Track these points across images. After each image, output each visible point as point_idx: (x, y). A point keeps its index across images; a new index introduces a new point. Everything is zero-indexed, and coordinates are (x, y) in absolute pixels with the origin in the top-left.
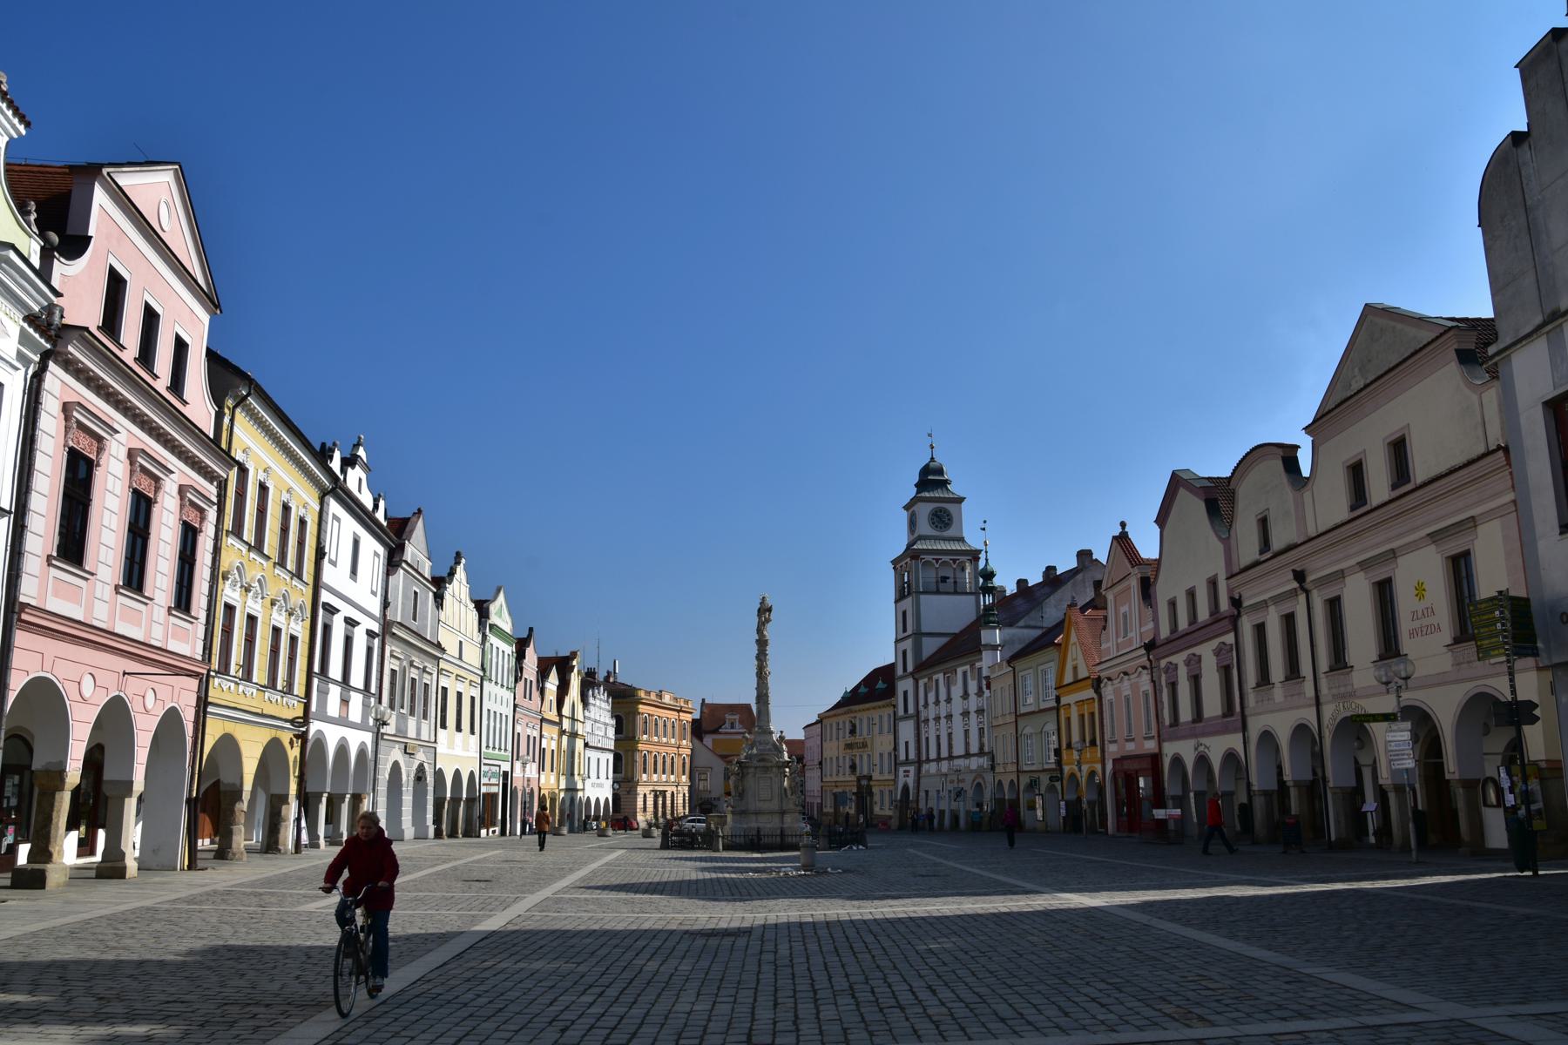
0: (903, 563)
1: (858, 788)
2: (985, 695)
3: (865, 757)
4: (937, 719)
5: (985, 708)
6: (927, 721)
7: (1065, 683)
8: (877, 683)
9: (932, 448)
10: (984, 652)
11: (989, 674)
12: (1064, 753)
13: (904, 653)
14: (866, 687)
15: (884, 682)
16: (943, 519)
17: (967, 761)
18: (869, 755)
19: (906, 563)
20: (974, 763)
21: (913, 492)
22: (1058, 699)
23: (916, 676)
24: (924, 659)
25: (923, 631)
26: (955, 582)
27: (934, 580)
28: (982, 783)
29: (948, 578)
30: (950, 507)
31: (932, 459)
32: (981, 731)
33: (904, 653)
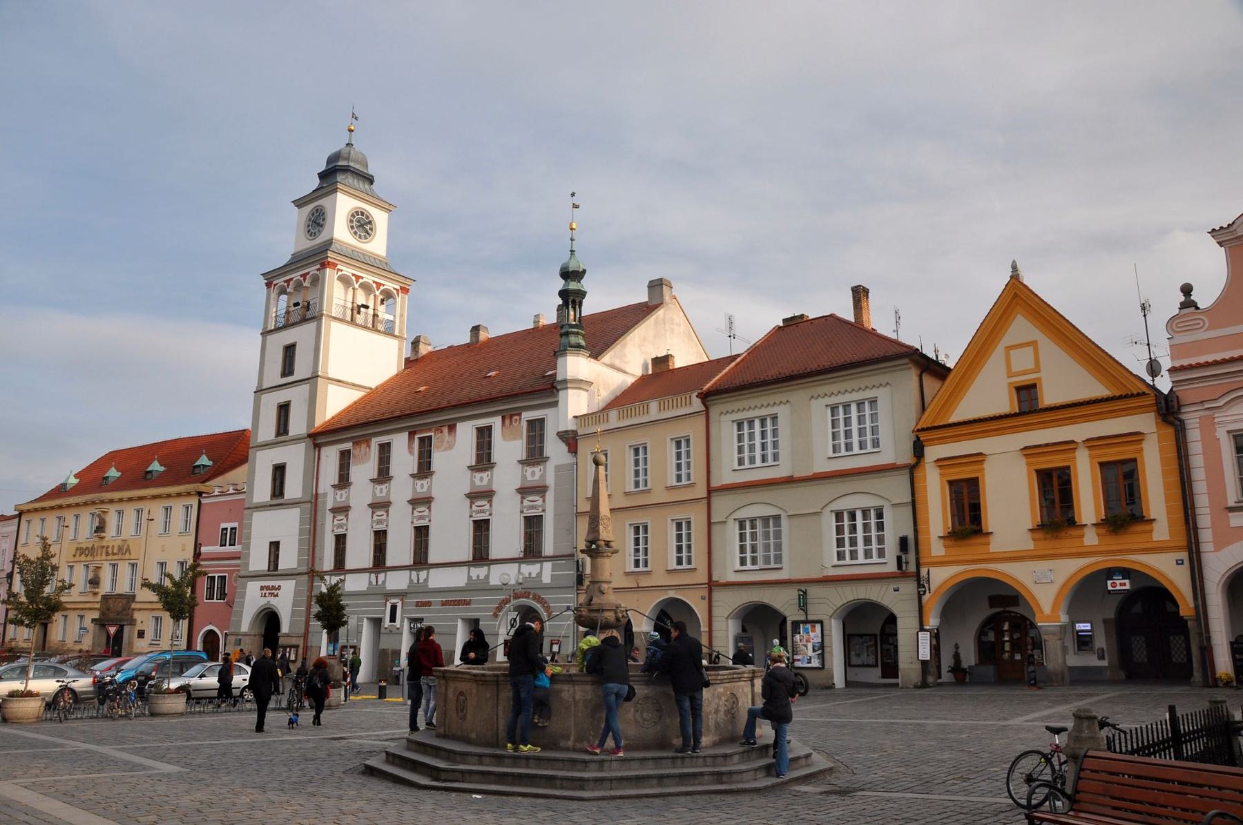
0: (296, 276)
1: (103, 614)
2: (550, 467)
4: (380, 506)
5: (550, 481)
7: (953, 419)
8: (150, 463)
10: (560, 392)
11: (573, 427)
12: (937, 549)
13: (284, 409)
15: (161, 465)
16: (362, 225)
17: (479, 572)
19: (304, 276)
20: (498, 575)
21: (315, 182)
22: (919, 450)
24: (329, 416)
26: (375, 315)
28: (538, 607)
29: (367, 307)
32: (533, 525)
33: (284, 409)
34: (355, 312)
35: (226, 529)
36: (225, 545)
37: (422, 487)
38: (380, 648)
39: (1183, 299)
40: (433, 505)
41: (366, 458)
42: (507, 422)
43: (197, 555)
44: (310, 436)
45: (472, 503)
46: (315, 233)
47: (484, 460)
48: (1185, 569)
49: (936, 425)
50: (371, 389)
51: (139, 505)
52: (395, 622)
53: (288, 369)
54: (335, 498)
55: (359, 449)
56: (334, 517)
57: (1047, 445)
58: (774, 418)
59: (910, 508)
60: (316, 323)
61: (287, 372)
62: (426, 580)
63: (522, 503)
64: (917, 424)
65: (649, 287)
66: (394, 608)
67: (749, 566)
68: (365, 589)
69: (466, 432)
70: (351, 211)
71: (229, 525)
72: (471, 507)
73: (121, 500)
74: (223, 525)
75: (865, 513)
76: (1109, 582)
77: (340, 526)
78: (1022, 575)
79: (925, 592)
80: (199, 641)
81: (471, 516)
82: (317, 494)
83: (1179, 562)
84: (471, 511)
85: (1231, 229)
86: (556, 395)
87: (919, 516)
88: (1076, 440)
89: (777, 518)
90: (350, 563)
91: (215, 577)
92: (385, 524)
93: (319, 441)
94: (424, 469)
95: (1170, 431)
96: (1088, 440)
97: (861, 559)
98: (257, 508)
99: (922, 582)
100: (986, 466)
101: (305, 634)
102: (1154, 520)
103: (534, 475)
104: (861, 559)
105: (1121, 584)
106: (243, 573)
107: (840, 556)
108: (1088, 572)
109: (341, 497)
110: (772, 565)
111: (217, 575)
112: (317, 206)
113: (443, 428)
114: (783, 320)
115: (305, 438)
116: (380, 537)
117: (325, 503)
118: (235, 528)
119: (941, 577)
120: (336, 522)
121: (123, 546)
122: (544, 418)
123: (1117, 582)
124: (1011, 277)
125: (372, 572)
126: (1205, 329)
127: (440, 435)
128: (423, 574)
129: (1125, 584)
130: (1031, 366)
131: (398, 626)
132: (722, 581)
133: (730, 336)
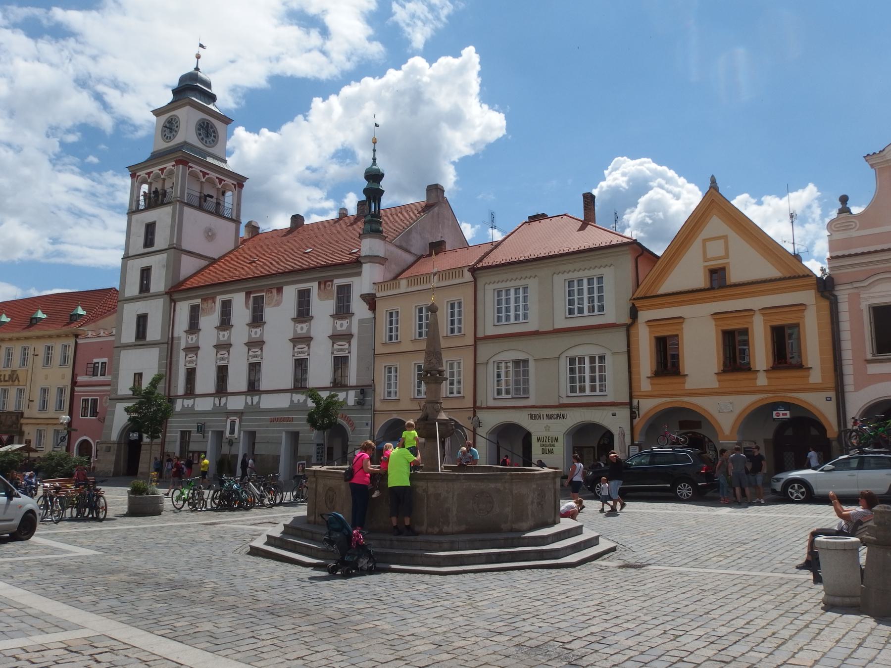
0: (156, 170)
2: (355, 320)
3: (13, 392)
4: (223, 347)
5: (355, 330)
6: (193, 349)
9: (198, 57)
11: (373, 292)
12: (645, 385)
14: (8, 316)
17: (299, 398)
18: (21, 391)
19: (162, 170)
21: (169, 97)
22: (634, 313)
23: (175, 296)
24: (182, 278)
25: (184, 248)
26: (218, 204)
27: (198, 194)
29: (211, 197)
30: (218, 124)
31: (197, 69)
32: (340, 363)
34: (202, 200)
35: (98, 363)
36: (97, 376)
37: (256, 333)
38: (222, 453)
39: (840, 206)
40: (265, 347)
41: (212, 310)
42: (322, 286)
43: (74, 383)
44: (167, 293)
45: (294, 346)
46: (170, 137)
47: (303, 313)
48: (832, 405)
49: (648, 295)
50: (214, 259)
51: (26, 344)
52: (234, 434)
53: (149, 241)
54: (187, 341)
55: (206, 304)
56: (186, 355)
57: (732, 312)
58: (525, 289)
59: (626, 356)
60: (172, 207)
61: (148, 243)
62: (259, 403)
63: (333, 346)
64: (633, 295)
65: (427, 190)
66: (233, 423)
67: (504, 396)
68: (210, 409)
69: (290, 293)
70: (200, 120)
71: (100, 360)
72: (294, 349)
73: (11, 339)
74: (95, 360)
75: (592, 360)
76: (774, 413)
77: (191, 362)
78: (709, 406)
79: (635, 418)
80: (75, 448)
81: (293, 356)
82: (172, 338)
83: (828, 399)
84: (294, 352)
85: (882, 154)
86: (361, 266)
87: (633, 362)
88: (754, 309)
89: (526, 362)
90: (198, 390)
91: (88, 399)
92: (227, 360)
93: (174, 298)
94: (257, 320)
95: (825, 304)
96: (763, 309)
97: (588, 392)
98: (124, 347)
99: (634, 410)
100: (686, 326)
101: (162, 443)
102: (811, 368)
103: (342, 326)
104: (588, 392)
105: (784, 414)
106: (113, 396)
107: (573, 390)
108: (760, 404)
109: (192, 339)
110: (522, 395)
111: (90, 398)
112: (171, 116)
113: (272, 290)
114: (529, 217)
115: (163, 295)
116: (222, 373)
117: (179, 344)
118: (105, 363)
119: (647, 406)
120: (188, 359)
121: (13, 375)
122: (350, 284)
123: (781, 413)
124: (710, 188)
125: (216, 397)
126: (856, 229)
127: (270, 295)
128: (256, 399)
129: (786, 414)
130: (722, 253)
131: (236, 437)
132: (484, 405)
133: (492, 227)
